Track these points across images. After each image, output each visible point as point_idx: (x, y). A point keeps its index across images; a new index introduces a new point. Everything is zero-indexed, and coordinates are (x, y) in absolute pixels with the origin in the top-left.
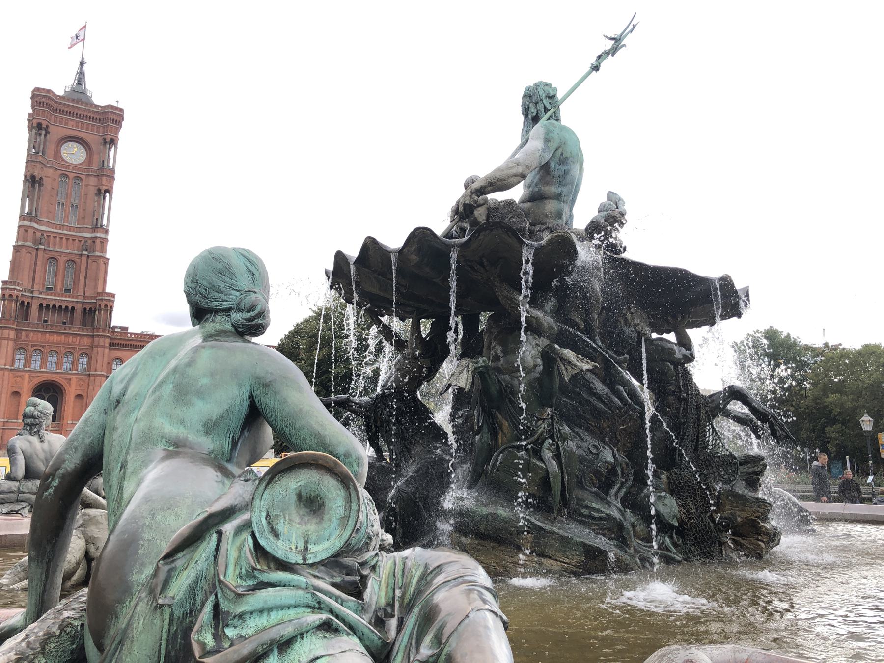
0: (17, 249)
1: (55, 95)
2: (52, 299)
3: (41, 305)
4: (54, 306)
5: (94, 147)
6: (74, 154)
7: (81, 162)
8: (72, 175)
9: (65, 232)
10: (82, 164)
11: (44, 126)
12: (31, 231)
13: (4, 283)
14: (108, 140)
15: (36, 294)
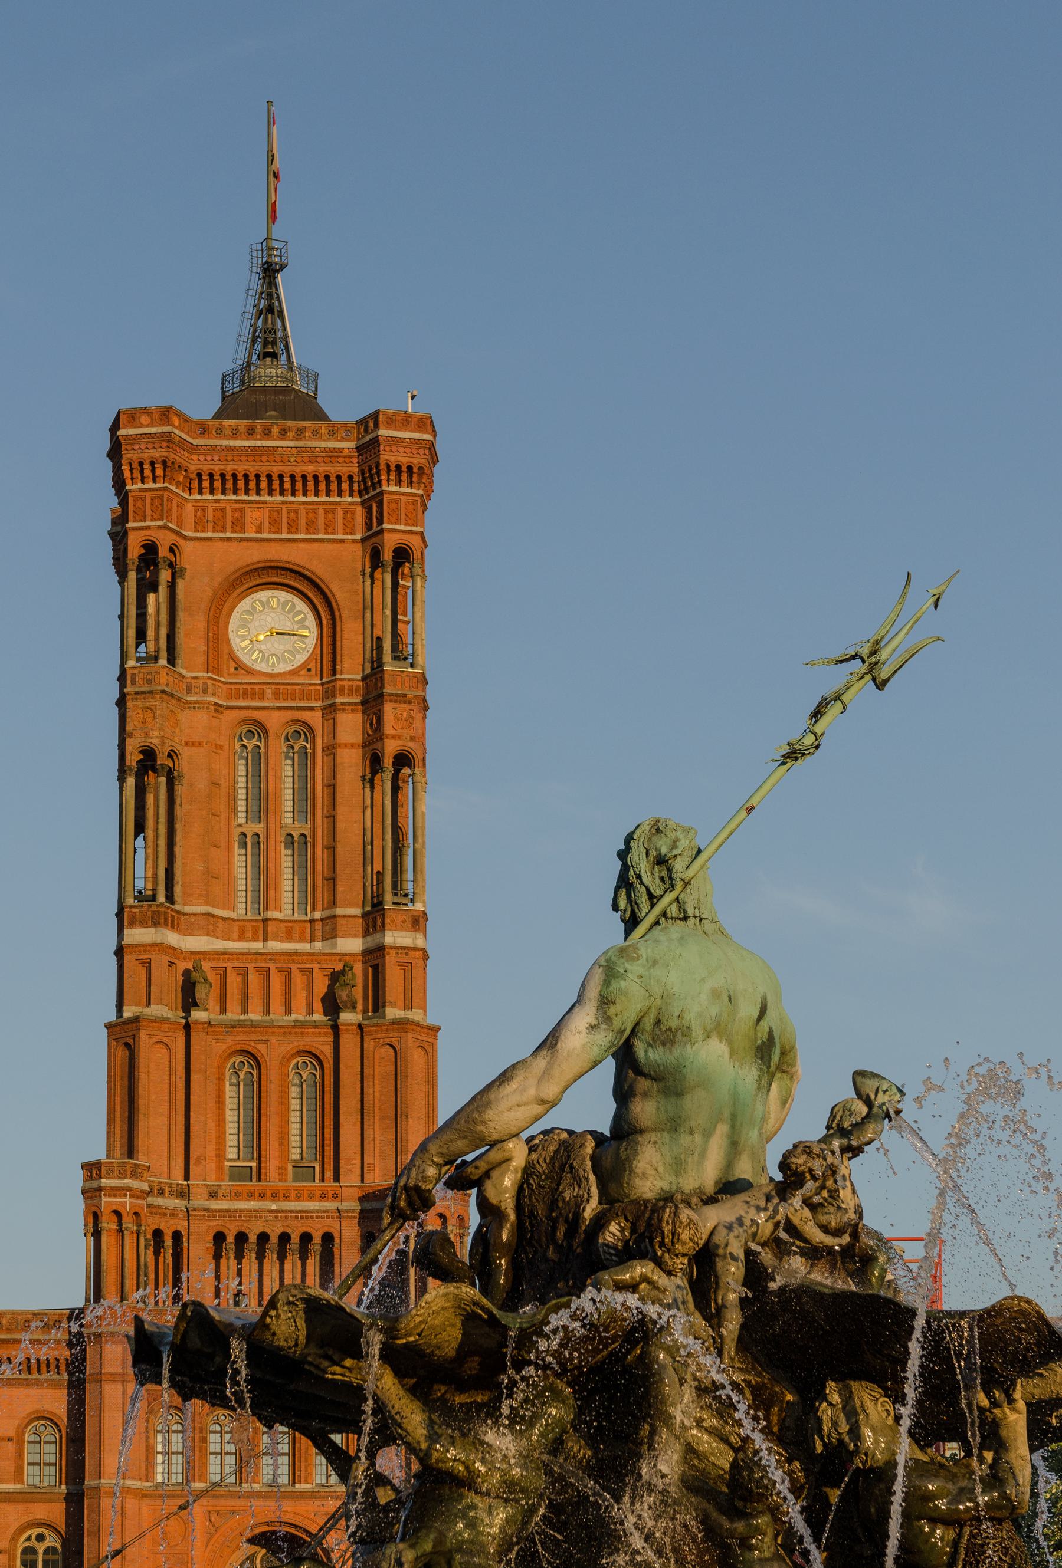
0: (124, 1035)
1: (185, 420)
2: (257, 1213)
3: (219, 1238)
4: (263, 1238)
5: (340, 592)
6: (271, 634)
7: (301, 659)
8: (274, 721)
9: (274, 946)
10: (305, 667)
11: (163, 552)
12: (159, 962)
13: (92, 1169)
14: (387, 556)
15: (199, 1201)
